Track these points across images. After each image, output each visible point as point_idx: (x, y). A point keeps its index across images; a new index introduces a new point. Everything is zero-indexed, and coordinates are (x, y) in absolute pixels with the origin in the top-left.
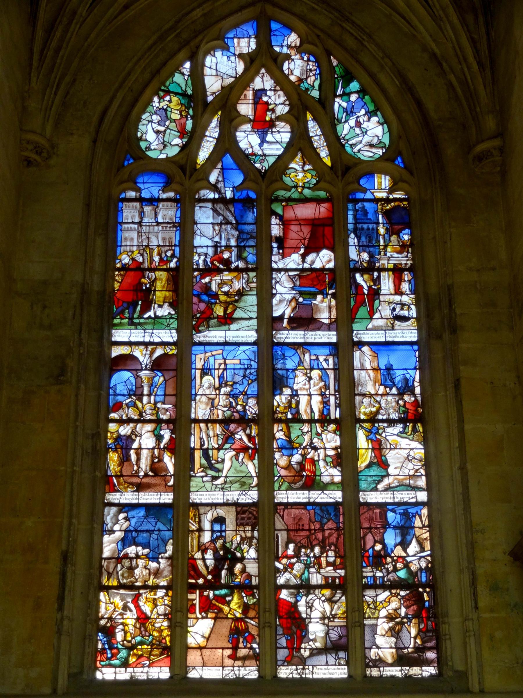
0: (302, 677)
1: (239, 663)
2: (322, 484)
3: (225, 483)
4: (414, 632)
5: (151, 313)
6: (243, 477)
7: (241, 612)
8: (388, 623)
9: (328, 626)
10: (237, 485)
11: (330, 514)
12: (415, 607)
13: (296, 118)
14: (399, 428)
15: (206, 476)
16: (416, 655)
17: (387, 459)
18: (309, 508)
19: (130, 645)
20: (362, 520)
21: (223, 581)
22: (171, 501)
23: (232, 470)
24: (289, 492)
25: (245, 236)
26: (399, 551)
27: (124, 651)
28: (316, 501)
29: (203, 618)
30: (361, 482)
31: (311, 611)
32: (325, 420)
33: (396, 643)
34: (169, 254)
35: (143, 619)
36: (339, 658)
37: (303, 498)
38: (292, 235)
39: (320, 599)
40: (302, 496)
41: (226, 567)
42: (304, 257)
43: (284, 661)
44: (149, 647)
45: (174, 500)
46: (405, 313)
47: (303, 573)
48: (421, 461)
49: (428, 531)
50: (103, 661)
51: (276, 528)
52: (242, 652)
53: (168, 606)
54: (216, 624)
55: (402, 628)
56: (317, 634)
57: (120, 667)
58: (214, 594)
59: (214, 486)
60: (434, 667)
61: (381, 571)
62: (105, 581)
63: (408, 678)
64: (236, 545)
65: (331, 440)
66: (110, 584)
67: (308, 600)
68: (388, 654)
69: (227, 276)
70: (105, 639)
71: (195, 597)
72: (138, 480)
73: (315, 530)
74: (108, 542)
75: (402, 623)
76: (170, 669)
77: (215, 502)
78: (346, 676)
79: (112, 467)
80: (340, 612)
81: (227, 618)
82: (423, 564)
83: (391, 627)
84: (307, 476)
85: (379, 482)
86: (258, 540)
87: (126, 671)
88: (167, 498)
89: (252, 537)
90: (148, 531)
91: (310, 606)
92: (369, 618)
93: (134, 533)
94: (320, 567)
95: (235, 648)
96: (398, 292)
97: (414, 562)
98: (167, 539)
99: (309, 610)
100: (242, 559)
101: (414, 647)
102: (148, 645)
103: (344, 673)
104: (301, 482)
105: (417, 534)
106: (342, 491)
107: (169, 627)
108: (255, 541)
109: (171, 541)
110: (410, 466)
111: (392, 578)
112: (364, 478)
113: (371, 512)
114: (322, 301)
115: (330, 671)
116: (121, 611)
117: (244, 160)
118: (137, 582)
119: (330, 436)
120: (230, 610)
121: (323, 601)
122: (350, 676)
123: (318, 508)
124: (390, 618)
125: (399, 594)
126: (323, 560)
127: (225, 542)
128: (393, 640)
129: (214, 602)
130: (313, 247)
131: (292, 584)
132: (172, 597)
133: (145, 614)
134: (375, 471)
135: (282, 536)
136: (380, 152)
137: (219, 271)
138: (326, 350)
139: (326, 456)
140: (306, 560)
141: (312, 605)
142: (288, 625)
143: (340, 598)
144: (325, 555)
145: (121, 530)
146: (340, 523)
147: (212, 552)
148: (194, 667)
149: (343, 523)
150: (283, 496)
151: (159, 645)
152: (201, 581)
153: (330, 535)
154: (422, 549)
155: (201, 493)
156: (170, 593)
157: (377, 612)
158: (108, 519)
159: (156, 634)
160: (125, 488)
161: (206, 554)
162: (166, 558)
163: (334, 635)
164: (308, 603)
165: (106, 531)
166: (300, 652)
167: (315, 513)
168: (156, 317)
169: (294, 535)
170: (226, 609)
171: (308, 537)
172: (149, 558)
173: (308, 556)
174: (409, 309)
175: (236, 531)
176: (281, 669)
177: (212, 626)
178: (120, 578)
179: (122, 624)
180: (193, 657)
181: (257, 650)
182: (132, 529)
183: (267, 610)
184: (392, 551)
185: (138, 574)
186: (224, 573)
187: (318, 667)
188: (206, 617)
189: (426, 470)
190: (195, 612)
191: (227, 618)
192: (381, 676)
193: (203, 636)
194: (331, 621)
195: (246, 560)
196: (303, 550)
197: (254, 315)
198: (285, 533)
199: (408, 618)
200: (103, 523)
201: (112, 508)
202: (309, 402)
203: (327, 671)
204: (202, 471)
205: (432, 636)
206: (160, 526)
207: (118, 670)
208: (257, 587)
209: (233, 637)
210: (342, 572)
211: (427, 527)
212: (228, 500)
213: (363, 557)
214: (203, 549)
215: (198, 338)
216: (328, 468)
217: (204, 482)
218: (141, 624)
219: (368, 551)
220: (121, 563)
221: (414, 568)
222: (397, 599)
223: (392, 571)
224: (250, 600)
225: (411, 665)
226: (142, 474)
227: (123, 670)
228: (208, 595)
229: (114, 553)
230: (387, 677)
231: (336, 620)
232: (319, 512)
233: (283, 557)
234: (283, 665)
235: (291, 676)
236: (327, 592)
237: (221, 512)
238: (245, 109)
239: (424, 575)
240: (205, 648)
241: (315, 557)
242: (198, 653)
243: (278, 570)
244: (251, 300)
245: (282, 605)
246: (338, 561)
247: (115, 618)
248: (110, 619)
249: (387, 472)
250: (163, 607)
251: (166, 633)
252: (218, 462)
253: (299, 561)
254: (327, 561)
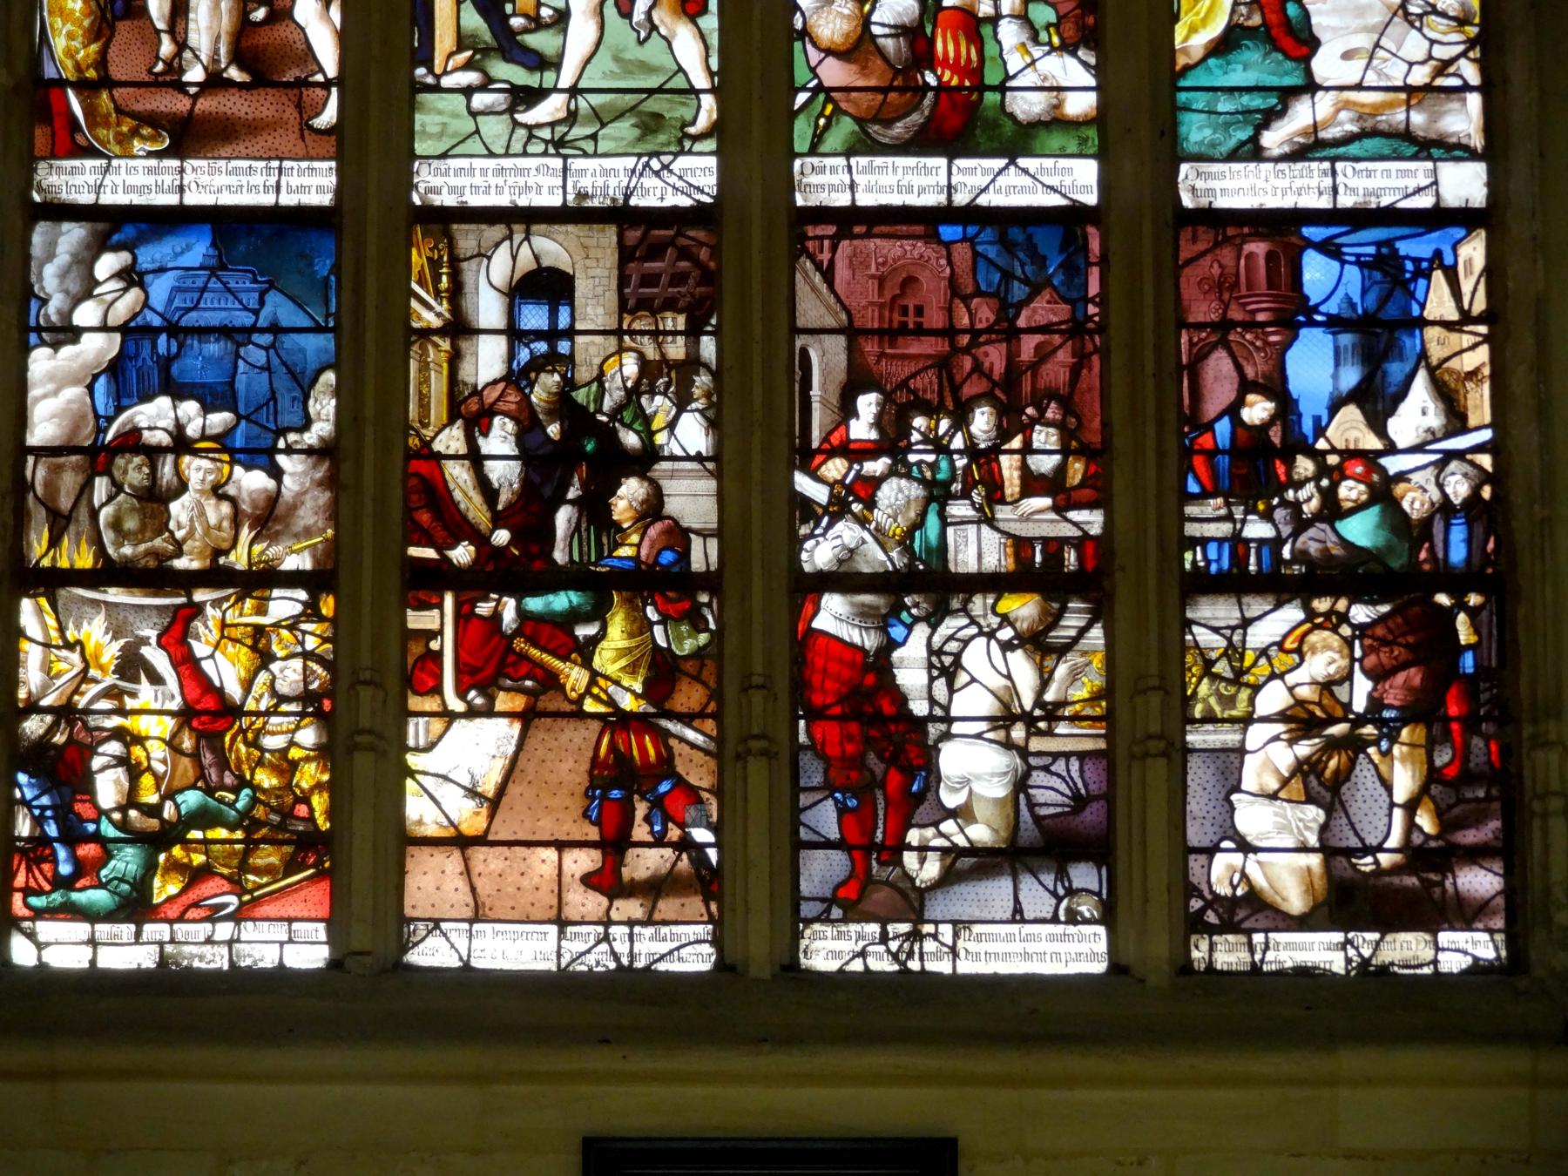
0: (905, 971)
1: (631, 908)
2: (1008, 127)
3: (572, 117)
4: (1404, 781)
6: (650, 92)
7: (638, 688)
8: (1292, 742)
9: (1024, 753)
10: (624, 129)
11: (1041, 262)
12: (1414, 676)
15: (483, 88)
16: (1411, 881)
17: (1307, 16)
18: (948, 232)
19: (154, 823)
20: (1189, 290)
21: (559, 556)
22: (326, 200)
23: (604, 61)
24: (860, 161)
26: (1350, 428)
27: (129, 851)
28: (983, 201)
29: (472, 713)
30: (1186, 118)
31: (952, 690)
33: (1324, 829)
35: (208, 714)
36: (1071, 892)
37: (922, 191)
39: (991, 635)
40: (918, 181)
41: (572, 493)
43: (830, 902)
44: (239, 835)
45: (339, 191)
47: (919, 523)
48: (1462, 21)
49: (1487, 339)
50: (39, 892)
51: (801, 323)
52: (646, 862)
53: (320, 660)
54: (528, 746)
55: (1353, 762)
56: (978, 788)
57: (110, 916)
58: (522, 613)
59: (521, 133)
60: (1491, 931)
61: (1267, 516)
62: (37, 545)
63: (1371, 975)
64: (619, 395)
66: (64, 563)
67: (937, 640)
68: (1288, 877)
70: (45, 800)
71: (437, 621)
72: (181, 105)
73: (974, 333)
74: (51, 377)
75: (1354, 745)
76: (329, 931)
77: (523, 202)
78: (1099, 967)
79: (59, 44)
80: (1080, 693)
81: (580, 715)
82: (1458, 488)
83: (1307, 760)
84: (942, 88)
85: (1269, 117)
86: (716, 375)
87: (138, 934)
88: (312, 184)
89: (693, 363)
90: (225, 332)
91: (946, 668)
92: (1210, 718)
93: (163, 338)
94: (995, 494)
95: (615, 844)
97: (1415, 477)
98: (312, 366)
99: (940, 688)
100: (646, 460)
101: (1406, 847)
102: (232, 828)
103: (1093, 956)
104: (916, 118)
105: (1436, 353)
106: (1101, 156)
107: (323, 752)
108: (703, 380)
109: (329, 377)
110: (1414, 45)
111: (1313, 548)
112: (1199, 101)
113: (1227, 255)
115: (1031, 947)
116: (111, 679)
118: (179, 553)
120: (593, 682)
121: (1006, 647)
122: (1117, 966)
123: (988, 234)
124: (1299, 721)
125: (1344, 618)
126: (1008, 465)
127: (569, 384)
128: (1314, 814)
129: (520, 644)
131: (866, 569)
132: (334, 621)
133: (220, 692)
134: (1253, 68)
135: (826, 359)
140: (933, 467)
141: (957, 663)
142: (850, 748)
143: (1082, 631)
144: (1016, 443)
145: (104, 328)
146: (1087, 300)
147: (510, 426)
148: (437, 923)
149: (1103, 300)
150: (826, 181)
151: (281, 827)
152: (462, 554)
153: (1044, 354)
154: (1457, 421)
155: (464, 163)
156: (327, 606)
157: (1244, 694)
158: (50, 278)
159: (265, 779)
160: (123, 140)
161: (485, 434)
162: (309, 451)
163: (1050, 793)
164: (940, 652)
165: (39, 329)
166: (899, 863)
167: (976, 255)
169: (882, 355)
170: (575, 677)
171: (943, 365)
172: (232, 451)
173: (941, 447)
175: (618, 332)
176: (813, 938)
177: (511, 749)
178: (108, 537)
179: (119, 734)
180: (431, 881)
181: (712, 854)
182: (157, 321)
183: (756, 680)
184: (1320, 431)
185: (184, 519)
186: (564, 517)
187: (977, 928)
188: (489, 712)
189: (1483, 65)
190: (437, 690)
191: (580, 715)
192: (1256, 969)
193: (472, 792)
194: (1040, 733)
195: (665, 465)
196: (919, 422)
198: (836, 346)
199: (1380, 723)
200: (27, 293)
201: (66, 226)
203: (1017, 947)
204: (468, 66)
205: (1488, 798)
206: (279, 308)
207: (103, 930)
208: (709, 581)
209: (604, 798)
210: (1092, 520)
211: (1478, 320)
212: (581, 195)
213: (1187, 453)
214: (472, 413)
216: (1037, 52)
217: (474, 114)
218: (199, 735)
219: (1209, 427)
220: (107, 472)
221: (1414, 502)
222: (1335, 640)
223: (1318, 517)
224: (680, 639)
225: (1388, 924)
226: (195, 74)
227: (127, 930)
228: (496, 616)
229: (76, 428)
230: (1281, 973)
231: (1062, 728)
232: (992, 252)
233: (831, 453)
234: (824, 918)
235: (857, 966)
236: (1023, 608)
237: (552, 248)
239: (1458, 534)
240: (481, 840)
241: (971, 450)
242: (451, 862)
243: (806, 508)
245: (819, 662)
246: (1077, 470)
247: (87, 711)
248: (66, 713)
249: (1309, 73)
250: (297, 663)
251: (309, 775)
252: (537, 24)
253: (901, 469)
254: (1024, 468)
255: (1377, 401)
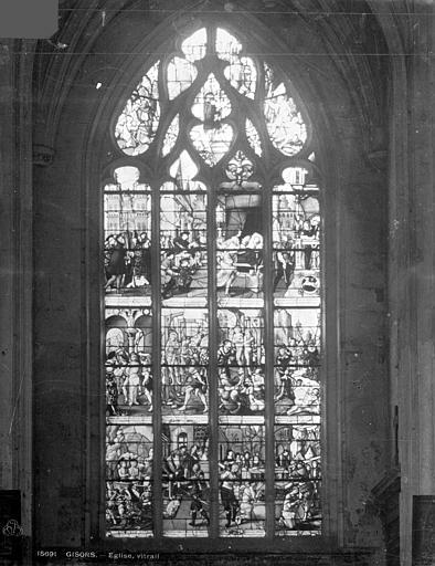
3: (187, 409)
5: (132, 284)
13: (236, 121)
14: (304, 370)
25: (198, 221)
32: (254, 365)
34: (143, 236)
38: (232, 221)
42: (240, 238)
46: (312, 284)
65: (258, 380)
69: (184, 255)
71: (168, 485)
91: (242, 492)
96: (308, 267)
114: (253, 275)
117: (197, 156)
119: (258, 377)
124: (291, 500)
130: (247, 231)
134: (287, 402)
136: (298, 149)
137: (181, 250)
138: (256, 313)
139: (254, 391)
168: (137, 287)
174: (315, 281)
197: (206, 286)
202: (243, 352)
210: (263, 471)
215: (165, 302)
237: (183, 429)
238: (198, 111)
244: (204, 272)
255: (303, 452)
